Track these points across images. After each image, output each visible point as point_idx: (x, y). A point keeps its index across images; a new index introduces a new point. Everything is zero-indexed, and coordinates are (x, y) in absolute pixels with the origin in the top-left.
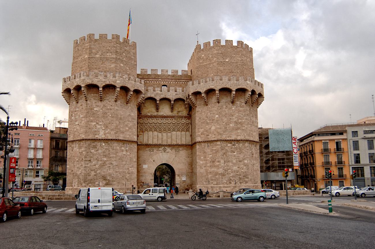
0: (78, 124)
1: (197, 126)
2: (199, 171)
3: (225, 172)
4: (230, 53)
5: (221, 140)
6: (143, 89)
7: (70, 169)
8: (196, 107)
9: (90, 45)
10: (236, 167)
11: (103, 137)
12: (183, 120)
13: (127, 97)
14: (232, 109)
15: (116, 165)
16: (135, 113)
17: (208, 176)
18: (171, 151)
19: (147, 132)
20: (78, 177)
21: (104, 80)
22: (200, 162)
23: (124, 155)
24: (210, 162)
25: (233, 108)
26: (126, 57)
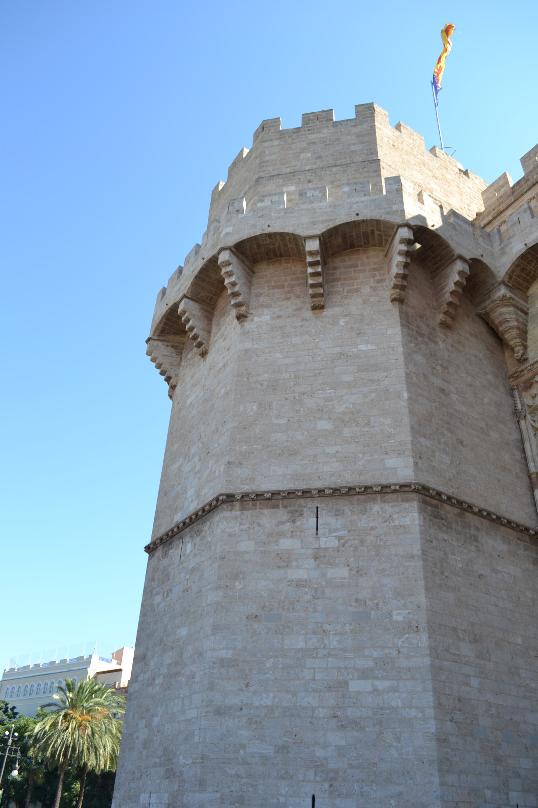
15: (223, 662)
23: (300, 584)
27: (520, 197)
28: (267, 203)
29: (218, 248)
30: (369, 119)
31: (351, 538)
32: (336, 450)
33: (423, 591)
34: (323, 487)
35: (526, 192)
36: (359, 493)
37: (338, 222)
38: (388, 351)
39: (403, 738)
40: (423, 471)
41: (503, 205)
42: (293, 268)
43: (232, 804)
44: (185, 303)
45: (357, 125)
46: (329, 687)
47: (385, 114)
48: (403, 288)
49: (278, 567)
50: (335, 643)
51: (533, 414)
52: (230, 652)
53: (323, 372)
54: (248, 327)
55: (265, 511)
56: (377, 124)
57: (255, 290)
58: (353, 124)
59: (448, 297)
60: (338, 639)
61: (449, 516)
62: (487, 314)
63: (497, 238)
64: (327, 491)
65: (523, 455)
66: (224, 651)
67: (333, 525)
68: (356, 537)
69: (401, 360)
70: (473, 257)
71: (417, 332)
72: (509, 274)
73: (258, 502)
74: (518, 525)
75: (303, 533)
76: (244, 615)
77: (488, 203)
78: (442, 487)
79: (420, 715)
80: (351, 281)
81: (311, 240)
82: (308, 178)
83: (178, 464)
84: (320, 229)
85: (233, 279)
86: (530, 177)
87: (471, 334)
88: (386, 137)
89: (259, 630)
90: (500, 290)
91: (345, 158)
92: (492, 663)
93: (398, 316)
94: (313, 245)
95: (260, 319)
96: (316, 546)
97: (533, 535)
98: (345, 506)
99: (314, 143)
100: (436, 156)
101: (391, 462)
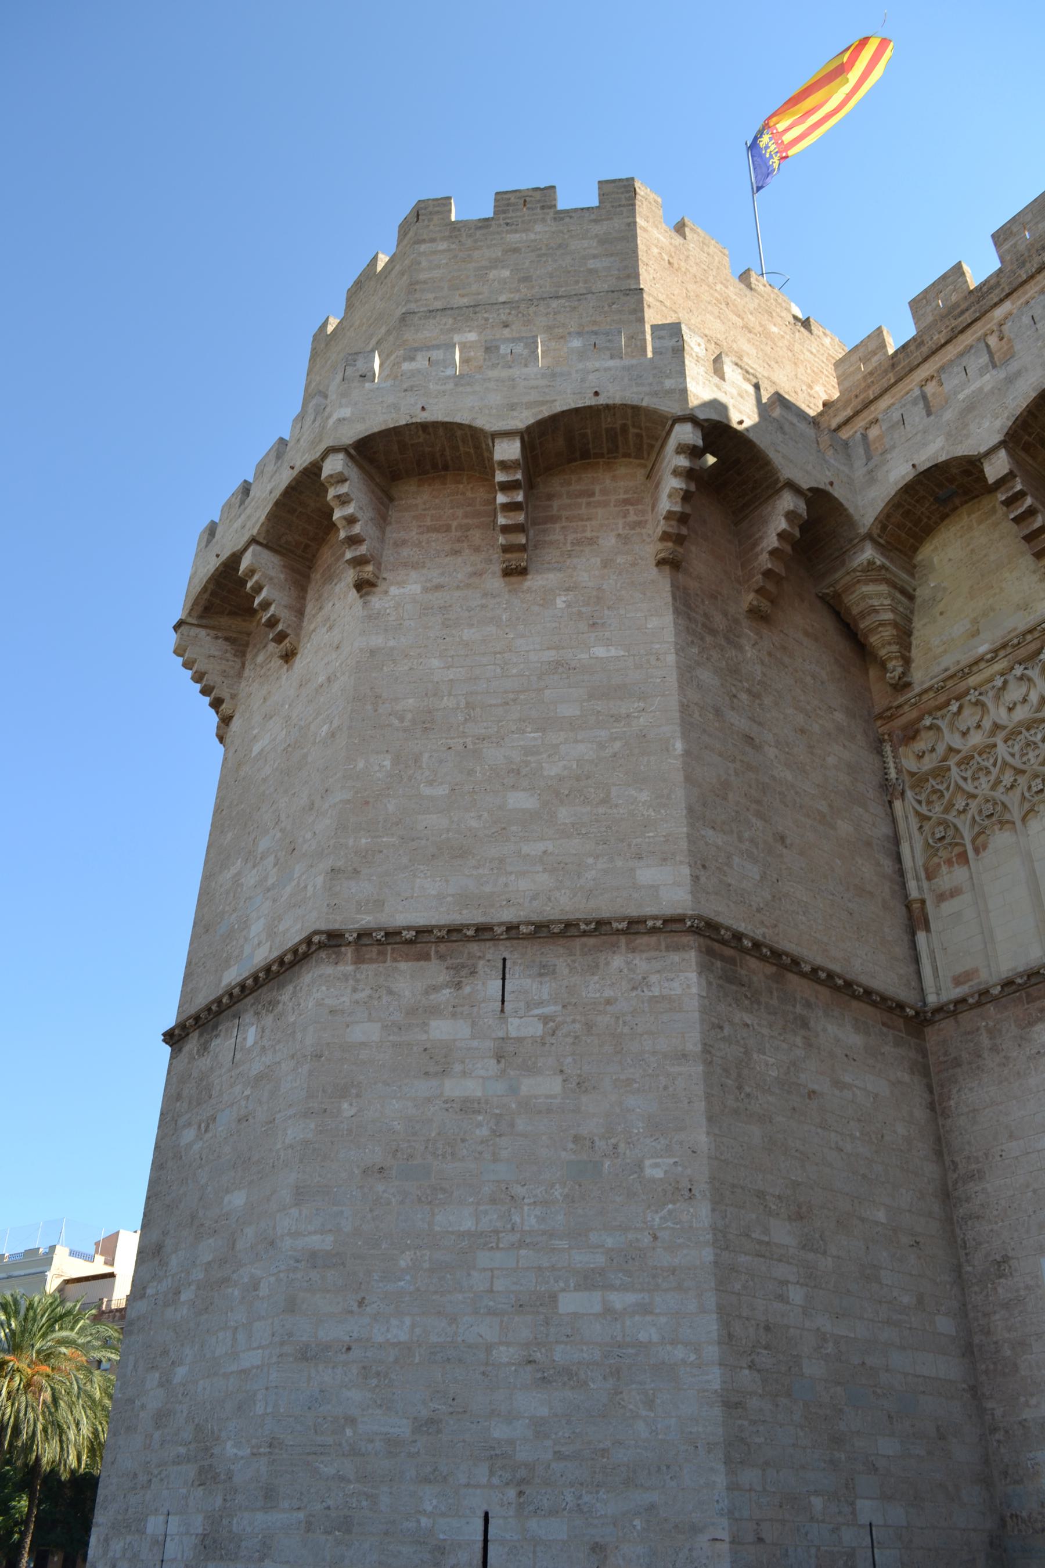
15: (314, 1258)
19: (1000, 839)
23: (467, 1107)
27: (906, 375)
28: (421, 362)
29: (323, 447)
30: (624, 209)
31: (569, 1019)
32: (544, 849)
33: (704, 1122)
34: (515, 920)
35: (919, 365)
36: (584, 934)
37: (559, 407)
38: (648, 661)
39: (659, 1401)
40: (708, 893)
41: (874, 388)
42: (469, 494)
43: (329, 1533)
44: (254, 555)
45: (602, 220)
46: (521, 1306)
47: (656, 201)
48: (679, 540)
49: (426, 1073)
50: (533, 1221)
51: (917, 790)
52: (330, 1238)
53: (522, 697)
54: (377, 606)
55: (403, 965)
56: (639, 220)
57: (393, 534)
58: (593, 217)
59: (764, 561)
60: (538, 1213)
61: (755, 979)
62: (838, 596)
63: (861, 451)
64: (523, 929)
65: (897, 867)
66: (316, 1238)
67: (535, 994)
68: (578, 1017)
69: (672, 680)
70: (814, 485)
71: (704, 625)
72: (881, 522)
73: (389, 948)
74: (884, 999)
75: (475, 1009)
76: (358, 1167)
77: (847, 384)
78: (743, 925)
79: (693, 1357)
80: (580, 523)
81: (505, 440)
82: (503, 317)
83: (233, 870)
84: (523, 419)
85: (350, 510)
86: (926, 338)
87: (806, 634)
88: (656, 246)
89: (385, 1195)
90: (862, 550)
91: (577, 282)
92: (830, 1259)
93: (669, 595)
94: (508, 450)
95: (402, 590)
96: (501, 1034)
97: (912, 1017)
98: (557, 957)
99: (516, 250)
100: (751, 289)
101: (648, 874)
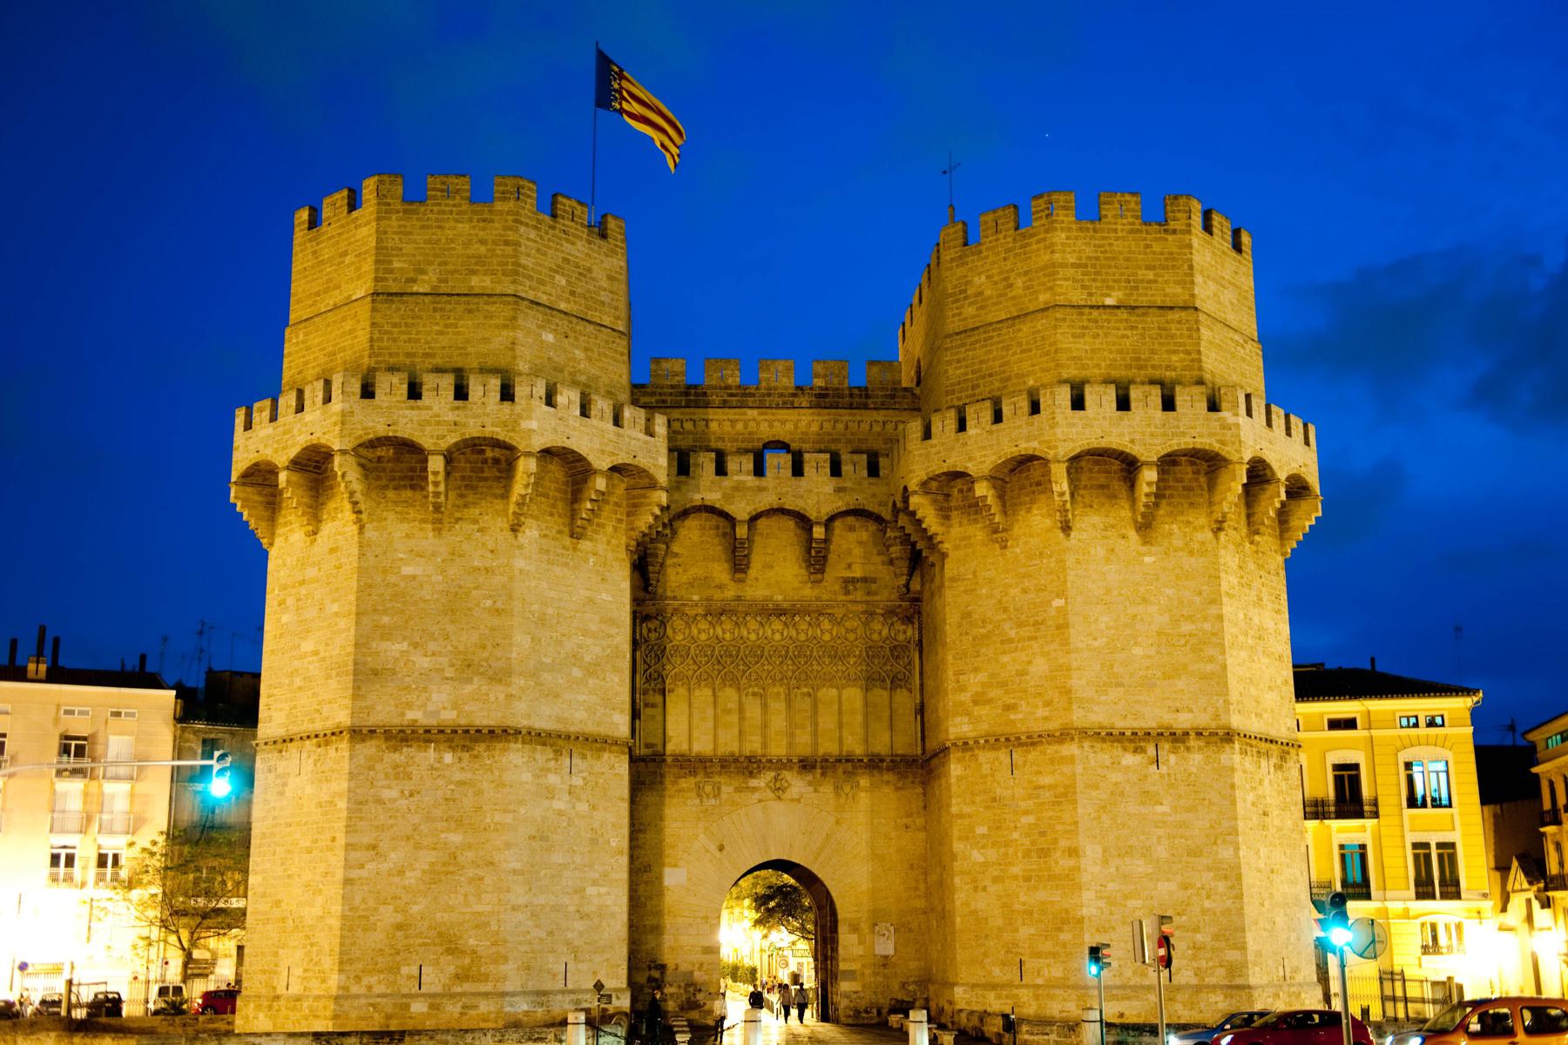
0: (316, 653)
1: (950, 658)
2: (967, 904)
3: (1111, 914)
4: (1128, 259)
5: (1084, 733)
6: (663, 461)
7: (264, 895)
8: (944, 556)
9: (381, 235)
10: (1173, 886)
11: (448, 716)
12: (877, 626)
13: (576, 506)
14: (1141, 563)
15: (515, 872)
16: (615, 593)
17: (1016, 930)
18: (816, 791)
19: (681, 691)
20: (307, 937)
21: (451, 417)
22: (969, 854)
23: (560, 813)
24: (1027, 854)
25: (1147, 559)
26: (573, 293)
